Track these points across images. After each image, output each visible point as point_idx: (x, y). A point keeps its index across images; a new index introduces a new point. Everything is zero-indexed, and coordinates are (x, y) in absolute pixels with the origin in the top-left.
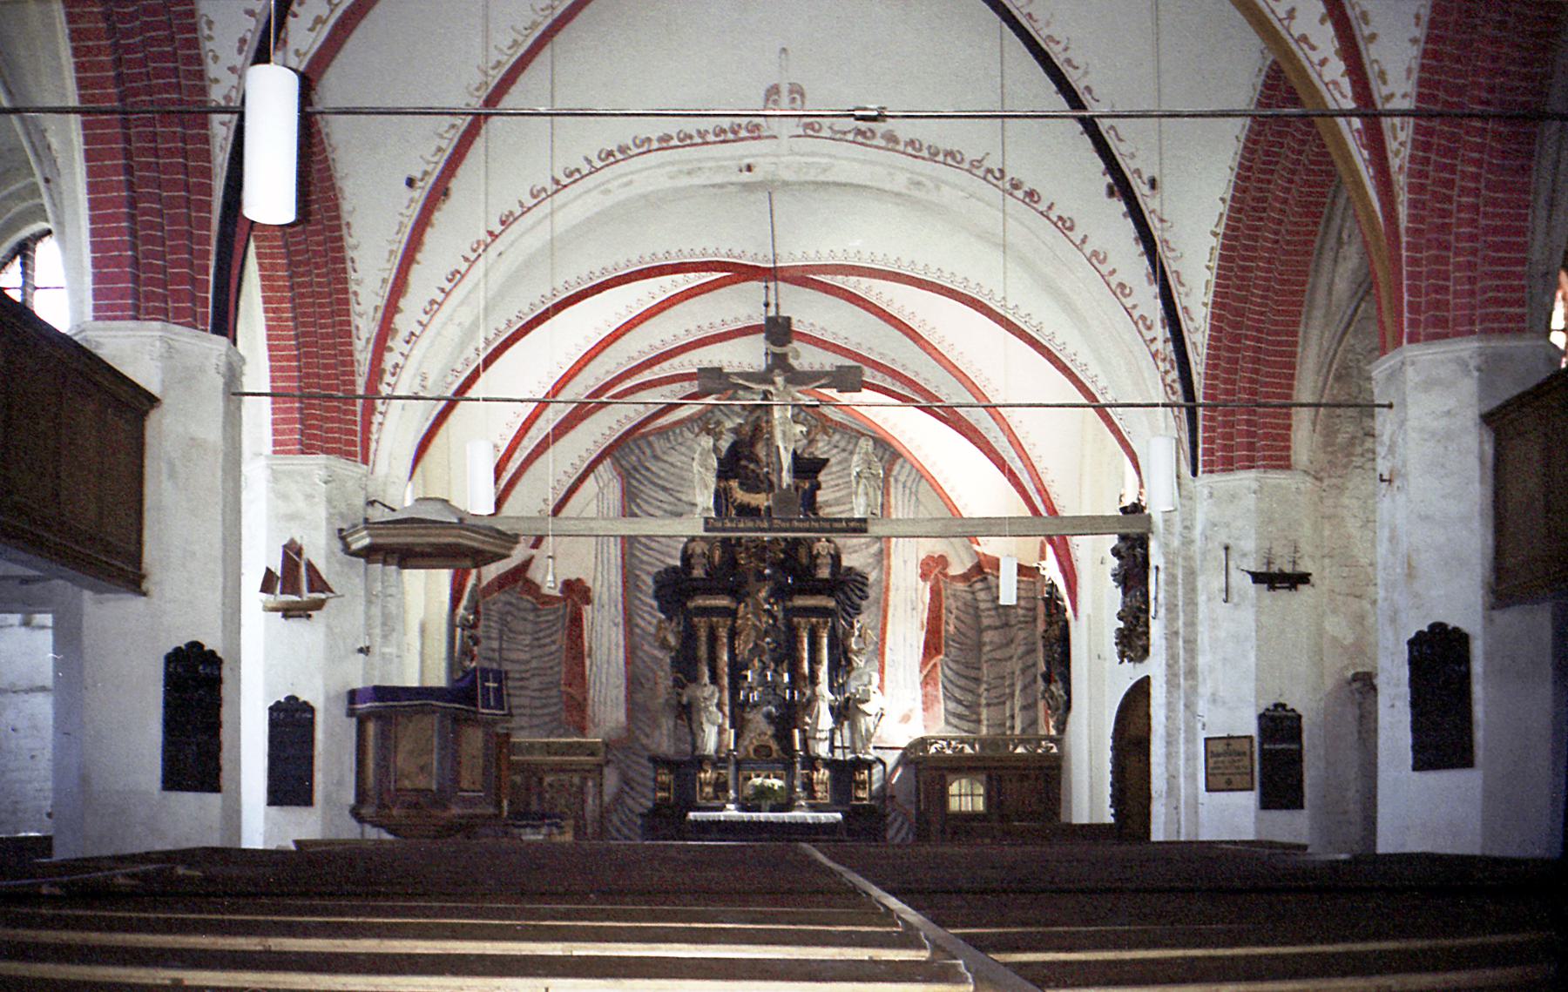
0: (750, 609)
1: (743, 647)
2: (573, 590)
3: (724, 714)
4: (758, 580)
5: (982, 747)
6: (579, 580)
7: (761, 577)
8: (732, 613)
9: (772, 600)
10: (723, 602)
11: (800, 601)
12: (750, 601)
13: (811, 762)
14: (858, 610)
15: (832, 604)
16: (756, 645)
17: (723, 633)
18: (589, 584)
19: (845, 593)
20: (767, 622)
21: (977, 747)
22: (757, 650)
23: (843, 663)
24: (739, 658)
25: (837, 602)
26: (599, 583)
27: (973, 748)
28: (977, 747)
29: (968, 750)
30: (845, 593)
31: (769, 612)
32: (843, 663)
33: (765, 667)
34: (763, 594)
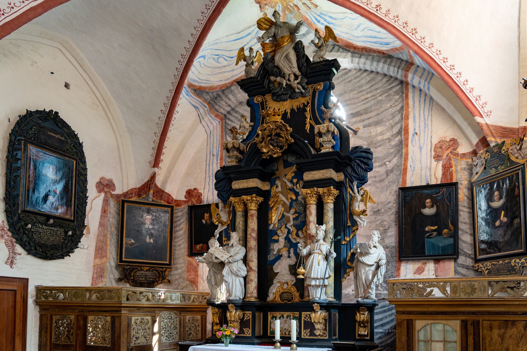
0: (279, 189)
1: (274, 217)
2: (192, 196)
3: (249, 269)
4: (285, 167)
5: (454, 290)
6: (195, 189)
7: (287, 165)
8: (266, 195)
9: (295, 181)
10: (254, 183)
11: (308, 176)
12: (278, 183)
13: (309, 306)
14: (363, 181)
15: (338, 177)
16: (283, 216)
17: (253, 208)
18: (201, 191)
19: (353, 168)
20: (291, 198)
21: (448, 289)
22: (283, 219)
23: (349, 224)
24: (271, 227)
25: (346, 176)
26: (206, 190)
27: (444, 291)
28: (448, 289)
29: (437, 293)
30: (353, 168)
31: (292, 190)
32: (349, 224)
33: (289, 232)
34: (290, 175)
